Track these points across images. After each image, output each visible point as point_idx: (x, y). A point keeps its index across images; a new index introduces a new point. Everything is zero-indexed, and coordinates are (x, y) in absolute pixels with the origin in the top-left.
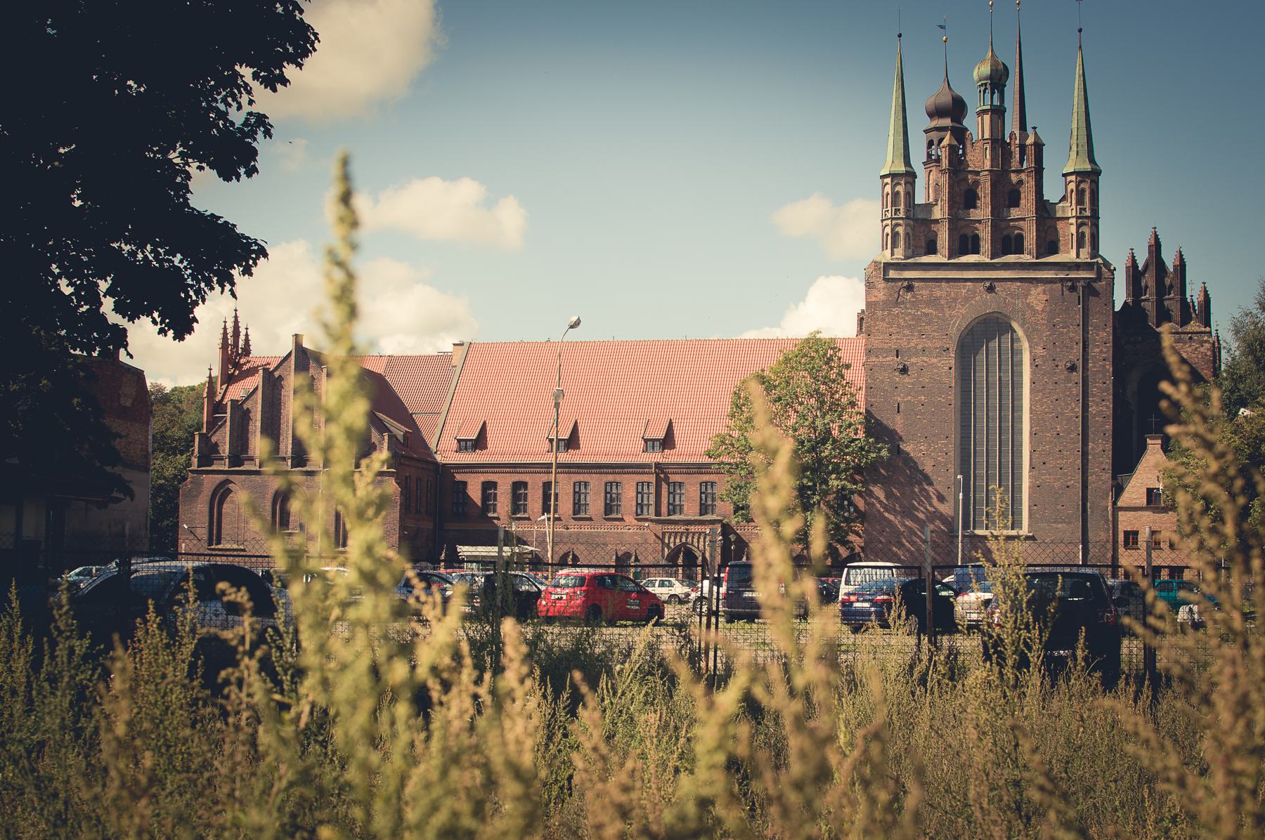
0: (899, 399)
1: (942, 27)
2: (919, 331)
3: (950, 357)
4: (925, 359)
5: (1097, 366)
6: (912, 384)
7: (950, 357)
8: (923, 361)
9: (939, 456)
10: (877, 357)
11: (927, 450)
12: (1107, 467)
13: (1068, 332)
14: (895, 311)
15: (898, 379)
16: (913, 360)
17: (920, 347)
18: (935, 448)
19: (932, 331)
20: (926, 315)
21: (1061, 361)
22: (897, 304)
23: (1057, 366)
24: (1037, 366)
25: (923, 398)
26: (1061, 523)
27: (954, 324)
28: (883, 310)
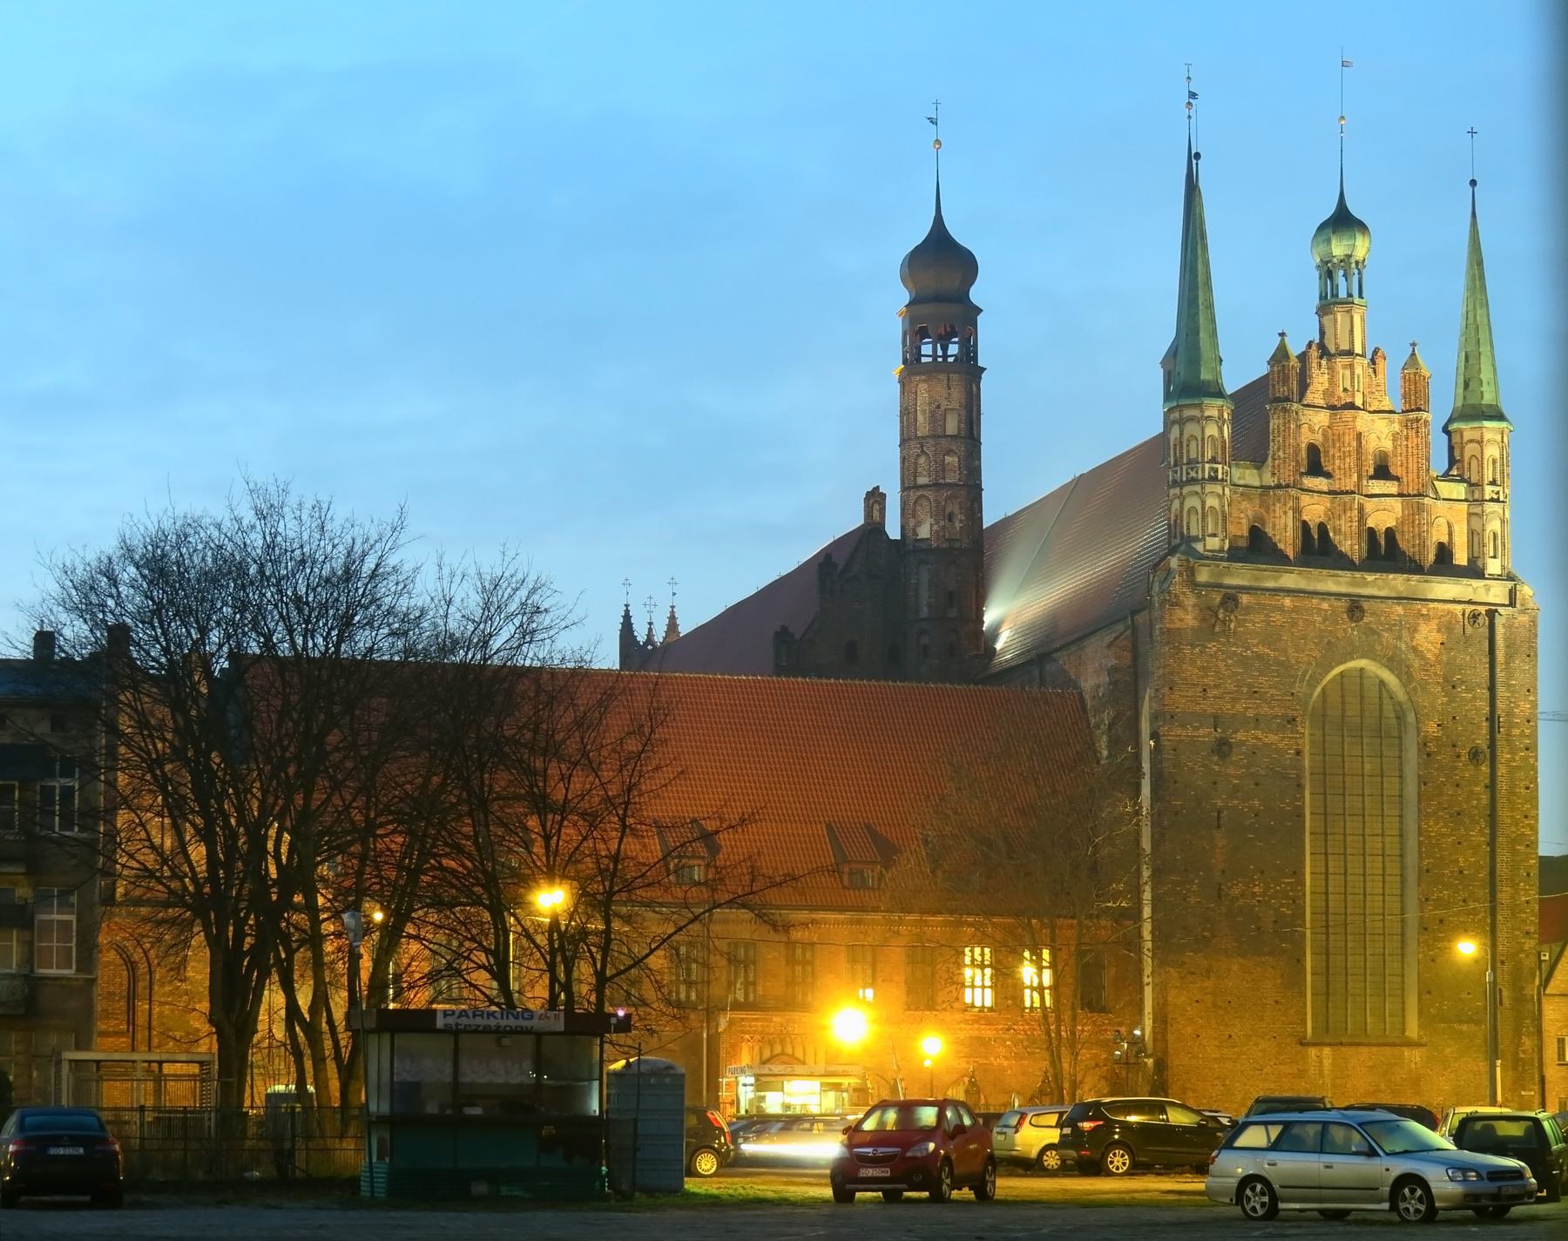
0: (1220, 803)
1: (933, 121)
2: (1250, 686)
3: (1297, 732)
4: (1259, 733)
5: (1517, 758)
6: (1240, 777)
7: (1297, 732)
8: (1257, 738)
9: (1282, 905)
10: (1183, 726)
11: (1264, 894)
12: (1532, 929)
13: (1474, 699)
14: (1212, 647)
15: (1217, 768)
16: (1240, 736)
17: (1250, 713)
18: (1276, 891)
19: (1270, 687)
20: (1259, 656)
21: (1464, 747)
22: (1213, 636)
23: (1458, 757)
24: (1429, 755)
25: (1257, 802)
26: (1467, 1023)
27: (1304, 675)
28: (1193, 646)
